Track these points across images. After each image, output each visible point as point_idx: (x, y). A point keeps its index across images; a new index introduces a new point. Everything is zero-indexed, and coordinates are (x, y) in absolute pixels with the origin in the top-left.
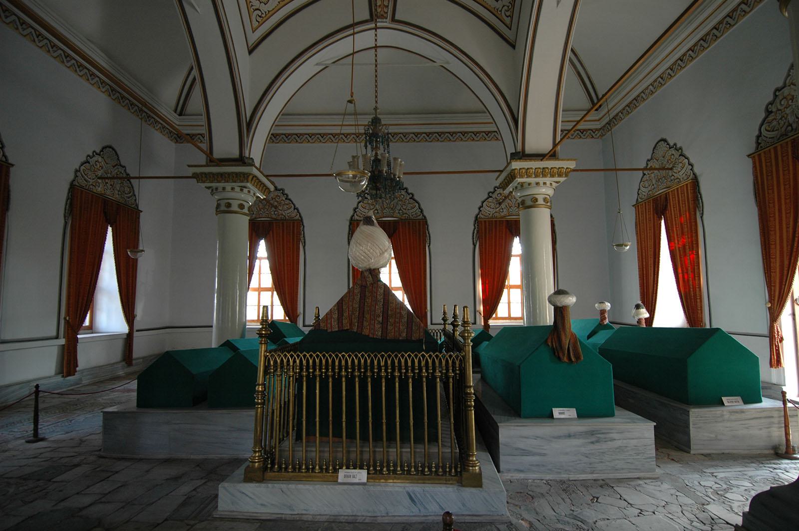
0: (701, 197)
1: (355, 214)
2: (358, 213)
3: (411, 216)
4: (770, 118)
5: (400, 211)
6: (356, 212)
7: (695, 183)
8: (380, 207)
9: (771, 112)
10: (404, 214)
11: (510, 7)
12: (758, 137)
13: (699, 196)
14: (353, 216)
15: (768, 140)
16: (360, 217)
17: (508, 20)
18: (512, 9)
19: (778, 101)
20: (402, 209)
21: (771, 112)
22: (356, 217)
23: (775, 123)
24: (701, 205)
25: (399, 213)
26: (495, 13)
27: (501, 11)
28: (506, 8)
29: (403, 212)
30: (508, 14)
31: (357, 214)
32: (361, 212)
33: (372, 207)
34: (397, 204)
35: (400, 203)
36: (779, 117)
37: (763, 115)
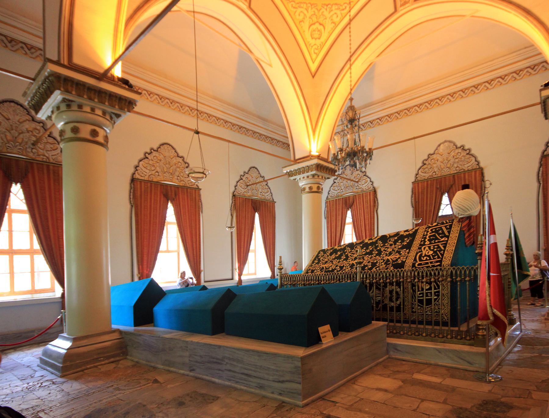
0: (377, 200)
1: (136, 172)
2: (139, 171)
3: (187, 184)
4: (425, 166)
5: (179, 178)
6: (137, 170)
7: (375, 192)
8: (160, 170)
9: (425, 164)
10: (181, 181)
11: (319, 48)
12: (417, 175)
13: (376, 199)
14: (134, 174)
15: (422, 177)
16: (141, 176)
17: (314, 56)
18: (320, 50)
19: (430, 159)
20: (180, 176)
21: (425, 164)
22: (137, 176)
23: (427, 169)
24: (377, 204)
25: (177, 179)
26: (308, 46)
27: (312, 47)
28: (316, 47)
29: (181, 179)
30: (316, 51)
31: (138, 173)
32: (142, 171)
33: (153, 168)
34: (176, 170)
35: (178, 169)
36: (429, 167)
37: (421, 165)
